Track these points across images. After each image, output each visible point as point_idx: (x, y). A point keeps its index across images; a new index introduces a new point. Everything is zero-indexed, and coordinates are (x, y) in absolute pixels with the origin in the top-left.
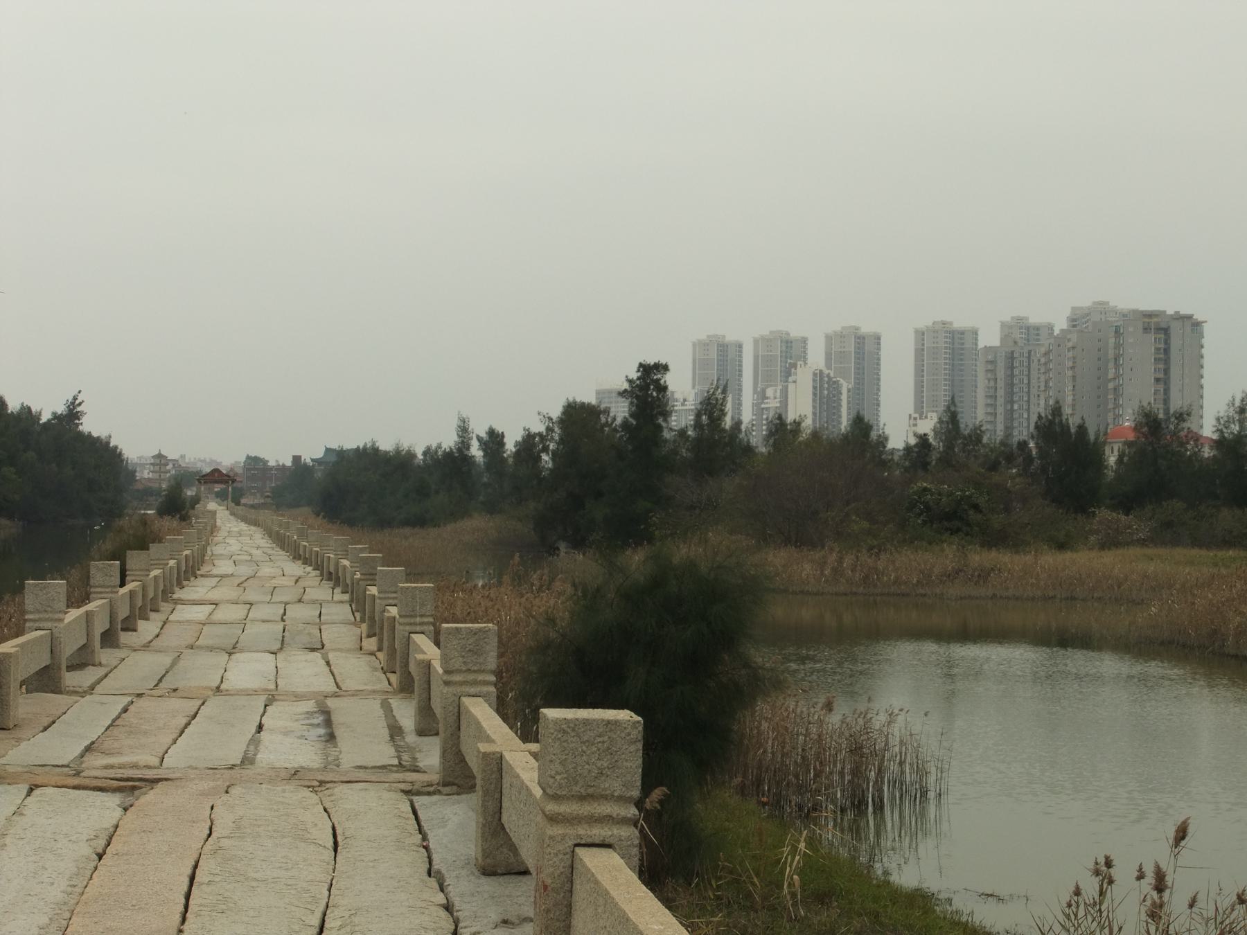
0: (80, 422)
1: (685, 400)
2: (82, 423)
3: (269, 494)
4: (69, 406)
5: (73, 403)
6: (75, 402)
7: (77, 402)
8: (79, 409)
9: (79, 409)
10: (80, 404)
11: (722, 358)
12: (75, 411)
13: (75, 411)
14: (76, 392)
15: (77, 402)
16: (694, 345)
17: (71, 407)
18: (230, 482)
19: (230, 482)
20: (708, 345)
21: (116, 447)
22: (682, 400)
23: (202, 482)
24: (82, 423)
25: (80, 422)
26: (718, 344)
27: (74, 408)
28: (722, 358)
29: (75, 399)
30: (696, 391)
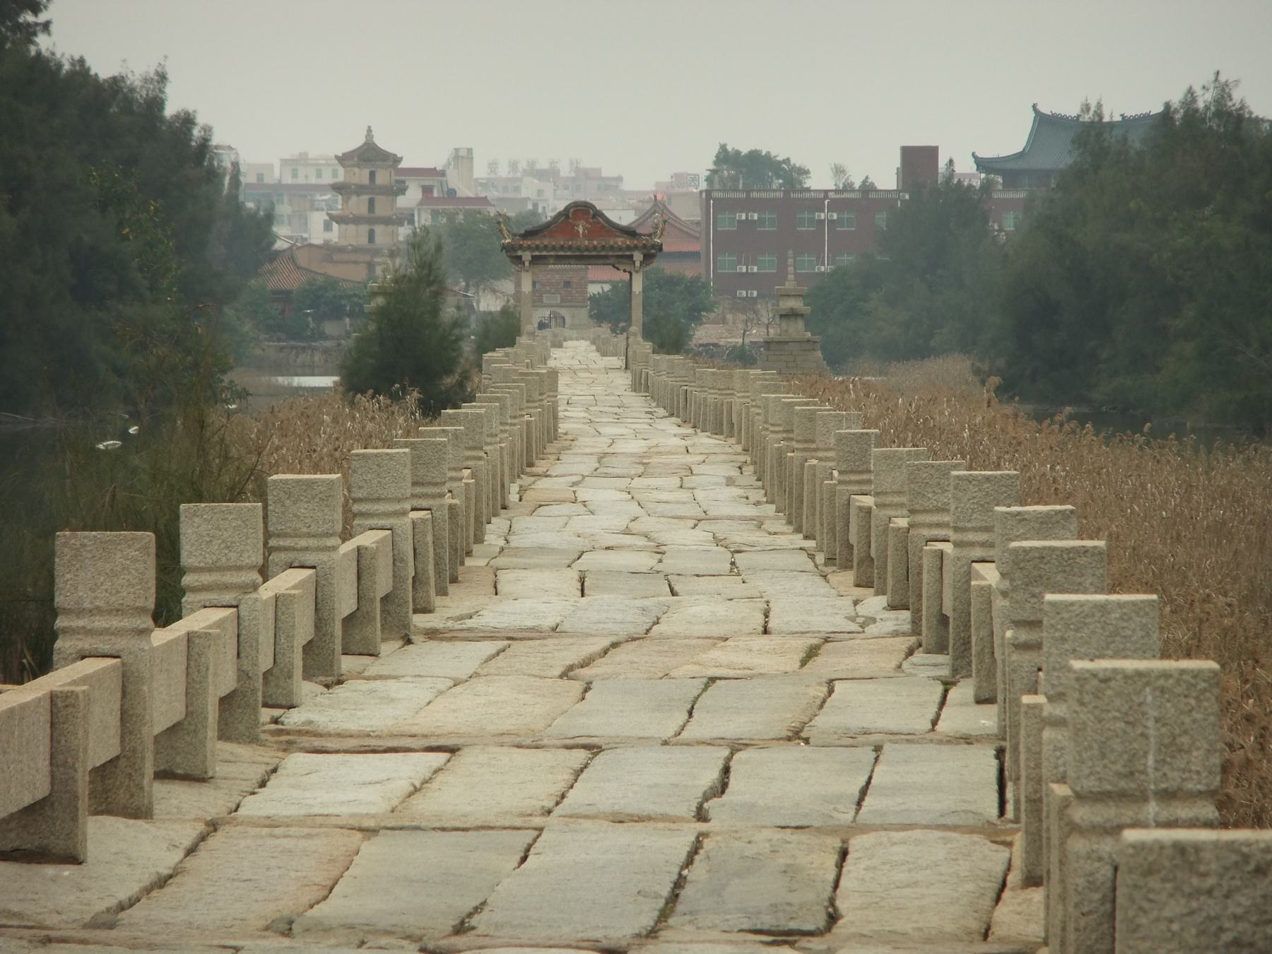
0: (42, 18)
2: (46, 26)
18: (638, 257)
19: (638, 257)
23: (527, 256)
24: (46, 26)
25: (42, 18)
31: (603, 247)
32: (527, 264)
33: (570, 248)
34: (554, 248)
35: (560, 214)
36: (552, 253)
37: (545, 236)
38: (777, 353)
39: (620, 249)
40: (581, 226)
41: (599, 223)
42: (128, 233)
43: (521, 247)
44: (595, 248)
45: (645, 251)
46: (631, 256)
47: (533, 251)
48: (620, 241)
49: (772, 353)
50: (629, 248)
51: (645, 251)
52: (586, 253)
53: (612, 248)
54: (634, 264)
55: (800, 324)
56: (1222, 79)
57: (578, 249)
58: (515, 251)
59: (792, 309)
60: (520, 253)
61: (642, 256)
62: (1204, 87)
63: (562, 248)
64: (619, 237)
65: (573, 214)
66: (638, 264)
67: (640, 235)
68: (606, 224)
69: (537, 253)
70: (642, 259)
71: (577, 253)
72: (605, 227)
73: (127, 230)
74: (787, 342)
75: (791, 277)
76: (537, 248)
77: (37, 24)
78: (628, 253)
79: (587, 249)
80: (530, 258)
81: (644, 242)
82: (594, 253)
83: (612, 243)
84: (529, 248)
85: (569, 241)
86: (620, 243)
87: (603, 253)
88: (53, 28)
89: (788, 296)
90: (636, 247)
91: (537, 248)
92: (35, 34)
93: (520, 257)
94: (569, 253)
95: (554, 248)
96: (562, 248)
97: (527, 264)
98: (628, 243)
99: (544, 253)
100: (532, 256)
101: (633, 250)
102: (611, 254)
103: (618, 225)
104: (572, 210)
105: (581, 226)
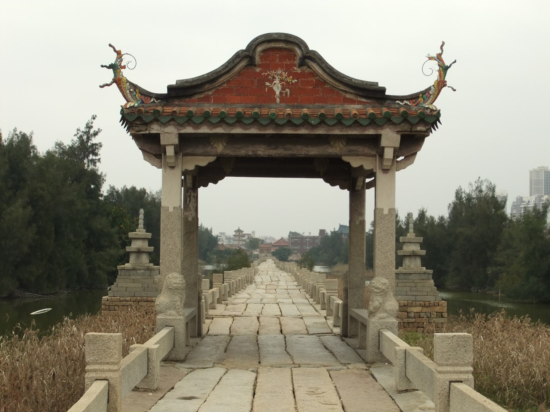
0: (97, 158)
1: (529, 202)
3: (416, 248)
4: (81, 136)
5: (87, 133)
6: (89, 132)
7: (92, 131)
8: (94, 140)
9: (94, 140)
10: (96, 134)
11: (547, 179)
12: (89, 144)
13: (89, 144)
14: (89, 118)
15: (92, 131)
16: (531, 172)
17: (85, 137)
20: (539, 172)
21: (141, 189)
22: (527, 202)
24: (99, 160)
26: (544, 172)
27: (88, 139)
28: (547, 179)
29: (89, 127)
30: (536, 196)
31: (323, 120)
32: (170, 151)
33: (256, 120)
34: (223, 120)
35: (239, 56)
36: (219, 130)
37: (207, 99)
38: (403, 281)
39: (356, 123)
40: (277, 81)
41: (314, 74)
42: (123, 227)
43: (157, 118)
44: (305, 121)
45: (406, 127)
46: (377, 139)
47: (182, 125)
48: (354, 109)
49: (401, 281)
50: (373, 121)
51: (406, 127)
52: (287, 131)
53: (339, 120)
54: (381, 155)
55: (418, 261)
56: (480, 180)
57: (272, 121)
58: (146, 124)
59: (413, 252)
60: (155, 129)
61: (398, 138)
62: (475, 182)
63: (239, 119)
64: (352, 102)
65: (261, 58)
66: (389, 154)
67: (394, 99)
68: (326, 77)
69: (189, 130)
70: (397, 145)
71: (270, 131)
72: (325, 82)
73: (122, 226)
74: (411, 274)
75: (411, 230)
76: (189, 119)
77: (96, 159)
78: (371, 132)
79: (290, 123)
80: (176, 141)
81: (402, 110)
82: (303, 131)
83: (338, 110)
84: (173, 119)
85: (253, 107)
86: (354, 112)
87: (321, 131)
88: (101, 160)
89: (410, 243)
90: (388, 120)
91: (189, 119)
92: (95, 163)
93: (156, 138)
94: (254, 131)
95: (223, 120)
96: (239, 119)
97: (170, 151)
98: (371, 111)
99: (204, 130)
100: (182, 137)
101: (381, 127)
102: (337, 132)
103: (351, 79)
104: (259, 49)
105: (277, 81)
